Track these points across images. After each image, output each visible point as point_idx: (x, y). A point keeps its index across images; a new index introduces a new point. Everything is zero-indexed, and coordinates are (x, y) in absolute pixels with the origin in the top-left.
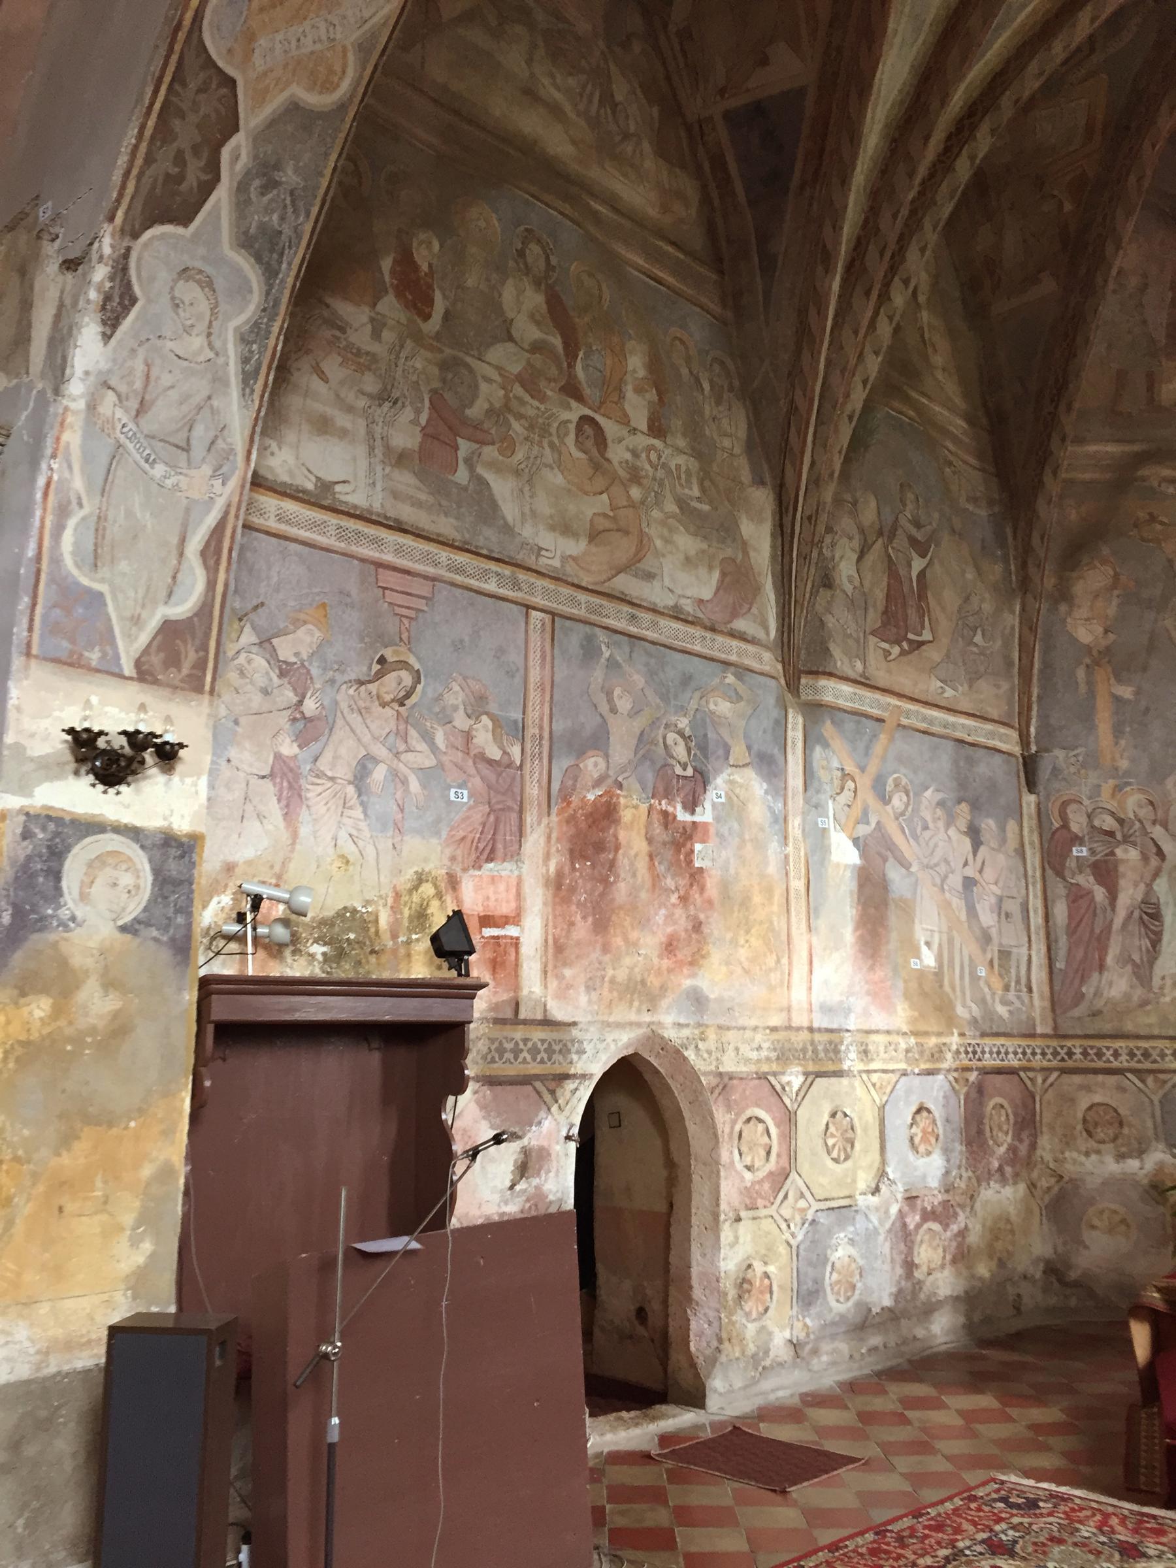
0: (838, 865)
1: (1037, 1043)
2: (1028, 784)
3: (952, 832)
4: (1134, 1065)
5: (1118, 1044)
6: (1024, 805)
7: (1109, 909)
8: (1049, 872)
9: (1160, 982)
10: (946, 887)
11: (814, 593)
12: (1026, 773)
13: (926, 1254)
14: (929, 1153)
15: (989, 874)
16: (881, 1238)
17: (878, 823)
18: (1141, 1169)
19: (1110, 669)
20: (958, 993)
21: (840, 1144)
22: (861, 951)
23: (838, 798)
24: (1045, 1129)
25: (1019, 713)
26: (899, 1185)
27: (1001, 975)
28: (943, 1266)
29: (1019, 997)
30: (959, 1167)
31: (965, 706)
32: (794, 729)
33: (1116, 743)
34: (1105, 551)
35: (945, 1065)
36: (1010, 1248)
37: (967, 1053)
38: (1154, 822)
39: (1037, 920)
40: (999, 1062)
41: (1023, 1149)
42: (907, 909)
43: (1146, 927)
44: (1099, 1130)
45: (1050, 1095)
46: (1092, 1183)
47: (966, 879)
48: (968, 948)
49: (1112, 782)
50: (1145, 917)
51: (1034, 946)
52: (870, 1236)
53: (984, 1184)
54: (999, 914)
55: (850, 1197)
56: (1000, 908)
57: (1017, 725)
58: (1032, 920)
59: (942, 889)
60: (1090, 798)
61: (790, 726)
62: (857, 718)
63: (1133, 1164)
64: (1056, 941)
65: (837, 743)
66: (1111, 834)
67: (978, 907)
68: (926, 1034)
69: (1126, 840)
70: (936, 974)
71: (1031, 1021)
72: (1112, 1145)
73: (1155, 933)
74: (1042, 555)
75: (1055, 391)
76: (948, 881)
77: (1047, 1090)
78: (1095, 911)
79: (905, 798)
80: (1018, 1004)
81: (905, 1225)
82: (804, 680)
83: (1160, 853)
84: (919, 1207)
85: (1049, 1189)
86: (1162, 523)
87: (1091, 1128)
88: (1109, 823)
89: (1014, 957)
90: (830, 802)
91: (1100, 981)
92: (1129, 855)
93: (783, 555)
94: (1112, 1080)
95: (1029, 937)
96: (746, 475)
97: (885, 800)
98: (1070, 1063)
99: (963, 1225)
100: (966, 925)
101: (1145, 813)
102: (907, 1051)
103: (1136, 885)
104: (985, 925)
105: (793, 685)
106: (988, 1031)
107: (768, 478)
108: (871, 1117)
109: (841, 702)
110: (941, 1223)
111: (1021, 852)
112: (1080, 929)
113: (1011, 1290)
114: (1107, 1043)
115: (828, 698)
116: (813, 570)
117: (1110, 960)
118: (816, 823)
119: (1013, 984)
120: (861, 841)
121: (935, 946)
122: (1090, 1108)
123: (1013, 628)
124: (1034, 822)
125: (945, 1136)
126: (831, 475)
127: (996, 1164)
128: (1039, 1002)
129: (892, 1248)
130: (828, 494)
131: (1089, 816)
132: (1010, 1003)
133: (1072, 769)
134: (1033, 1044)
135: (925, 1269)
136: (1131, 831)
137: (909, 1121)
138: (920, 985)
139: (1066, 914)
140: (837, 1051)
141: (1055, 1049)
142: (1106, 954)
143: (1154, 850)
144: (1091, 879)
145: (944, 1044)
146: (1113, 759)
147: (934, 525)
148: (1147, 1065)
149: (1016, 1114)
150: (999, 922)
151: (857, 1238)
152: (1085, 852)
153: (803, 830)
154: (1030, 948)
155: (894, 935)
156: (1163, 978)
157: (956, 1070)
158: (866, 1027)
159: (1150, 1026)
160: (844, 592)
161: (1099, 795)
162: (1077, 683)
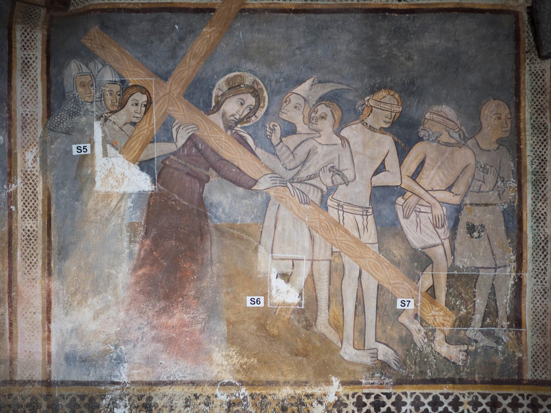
0: (108, 196)
6: (527, 78)
23: (113, 117)
51: (529, 265)
54: (454, 229)
56: (457, 222)
90: (97, 126)
119: (478, 317)
120: (156, 164)
132: (469, 341)
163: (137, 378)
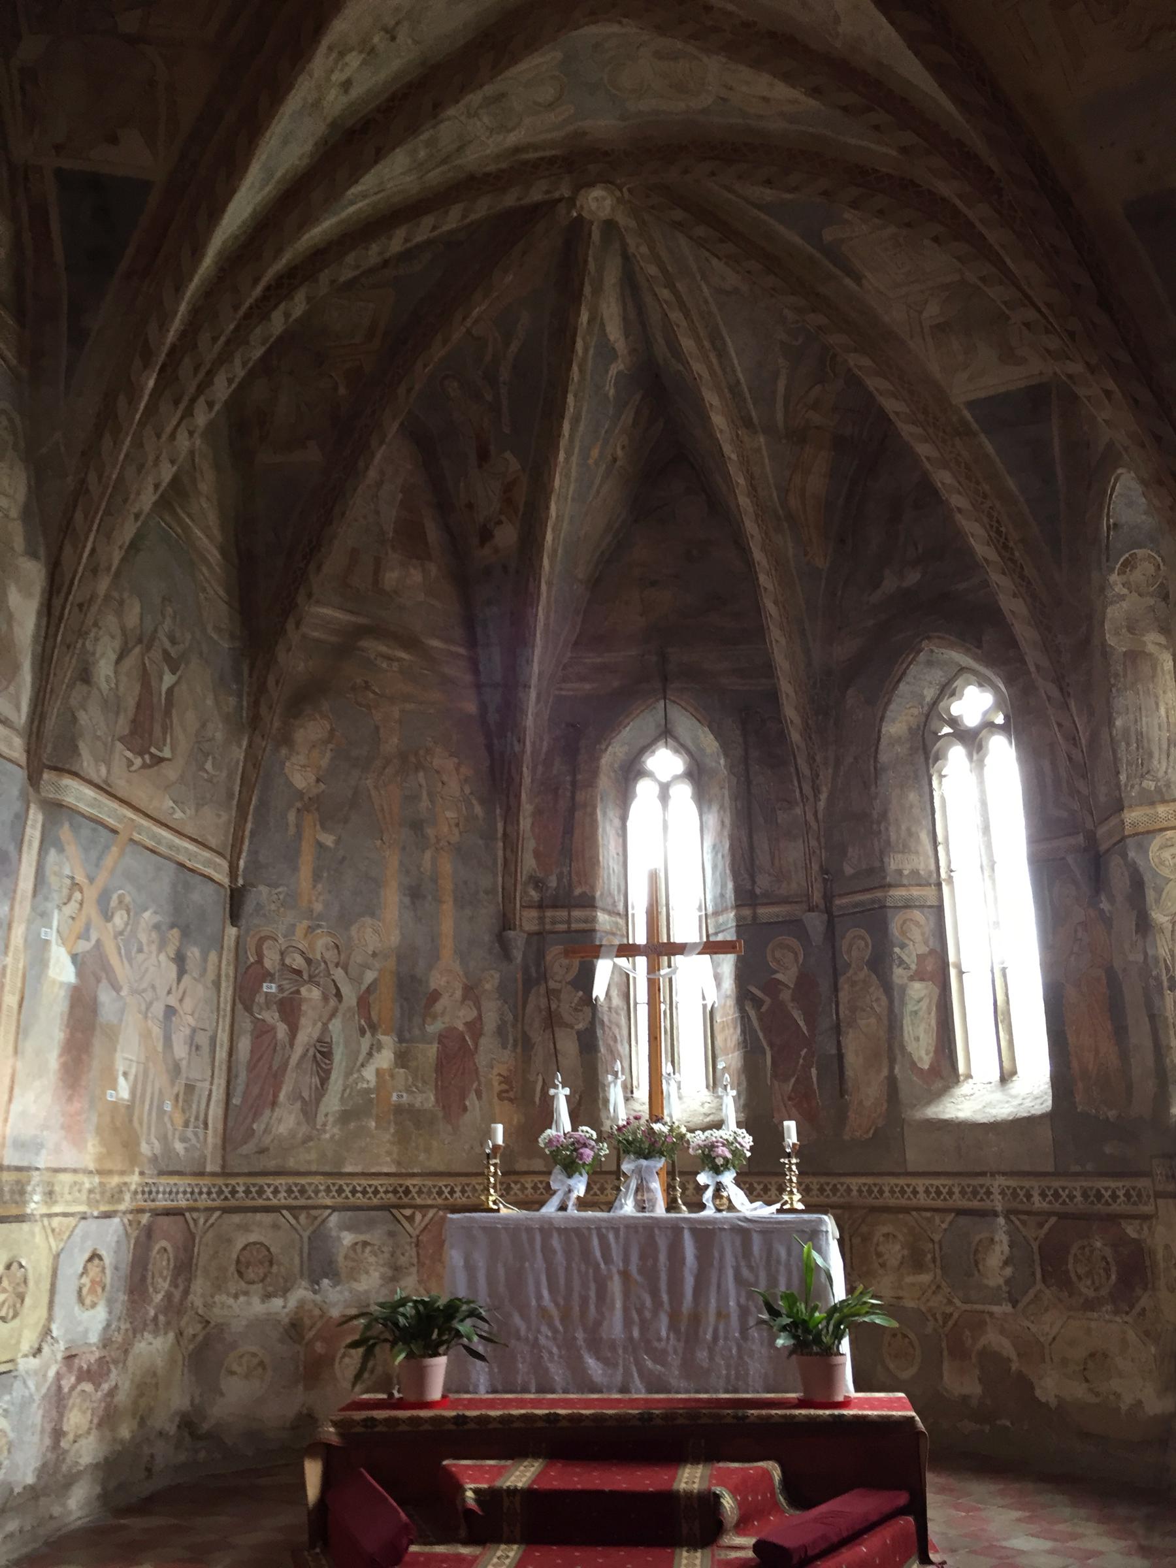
0: (54, 982)
1: (205, 1182)
2: (231, 917)
3: (162, 957)
4: (290, 1202)
5: (280, 1181)
7: (288, 1046)
8: (239, 1006)
9: (323, 1119)
10: (150, 1015)
11: (71, 686)
12: (231, 905)
13: (77, 1419)
14: (94, 1305)
15: (188, 1004)
16: (35, 1405)
17: (98, 941)
18: (284, 1307)
20: (145, 1126)
21: (10, 1302)
22: (61, 1079)
23: (64, 908)
24: (199, 1272)
25: (233, 846)
26: (61, 1342)
27: (183, 1111)
28: (89, 1432)
29: (196, 1134)
30: (120, 1318)
31: (189, 830)
32: (33, 827)
33: (314, 887)
35: (122, 1207)
36: (152, 1404)
37: (143, 1193)
38: (337, 965)
39: (222, 1054)
40: (169, 1203)
41: (177, 1295)
42: (112, 1035)
43: (318, 1065)
44: (250, 1270)
45: (210, 1234)
46: (237, 1326)
47: (168, 1006)
48: (159, 1080)
49: (305, 923)
50: (318, 1055)
51: (216, 1081)
52: (25, 1404)
53: (138, 1336)
54: (191, 1045)
55: (11, 1361)
58: (217, 1053)
59: (146, 1017)
60: (285, 937)
61: (29, 823)
62: (93, 825)
63: (278, 1302)
64: (237, 1076)
65: (72, 849)
66: (298, 972)
67: (174, 1037)
68: (110, 1173)
69: (312, 980)
70: (128, 1107)
71: (203, 1161)
72: (261, 1285)
73: (325, 1071)
76: (152, 1009)
77: (208, 1230)
78: (275, 1050)
79: (126, 916)
80: (194, 1141)
81: (60, 1388)
82: (46, 776)
83: (339, 995)
84: (76, 1366)
85: (194, 1336)
86: (374, 692)
87: (243, 1270)
88: (298, 962)
89: (197, 1092)
90: (56, 913)
91: (271, 1118)
92: (312, 994)
93: (46, 638)
94: (267, 1218)
95: (213, 1074)
96: (19, 543)
97: (108, 916)
98: (233, 1202)
99: (113, 1383)
100: (161, 1055)
101: (331, 955)
102: (91, 1191)
103: (314, 1024)
104: (177, 1057)
105: (34, 779)
106: (165, 1169)
107: (42, 551)
108: (45, 1267)
109: (83, 807)
110: (94, 1384)
111: (217, 984)
112: (261, 1064)
113: (146, 1450)
114: (269, 1180)
115: (70, 800)
116: (74, 661)
117: (282, 1096)
118: (39, 934)
119: (192, 1119)
120: (79, 958)
121: (131, 1078)
122: (244, 1248)
124: (232, 955)
125: (112, 1286)
126: (109, 569)
127: (152, 1313)
128: (212, 1138)
129: (43, 1416)
130: (103, 585)
131: (282, 954)
133: (273, 907)
134: (201, 1183)
135: (71, 1437)
136: (317, 972)
137: (80, 1270)
138: (113, 1118)
139: (249, 1048)
140: (22, 1192)
141: (220, 1187)
142: (280, 1088)
143: (334, 991)
144: (277, 1015)
145: (125, 1184)
146: (310, 901)
147: (187, 644)
148: (302, 1202)
149: (176, 1258)
150: (189, 1054)
151: (12, 1409)
152: (273, 988)
153: (26, 940)
154: (212, 1084)
155: (96, 1064)
156: (326, 1115)
157: (131, 1212)
158: (55, 1165)
159: (309, 1162)
160: (99, 689)
161: (294, 934)
162: (287, 824)
163: (49, 1165)
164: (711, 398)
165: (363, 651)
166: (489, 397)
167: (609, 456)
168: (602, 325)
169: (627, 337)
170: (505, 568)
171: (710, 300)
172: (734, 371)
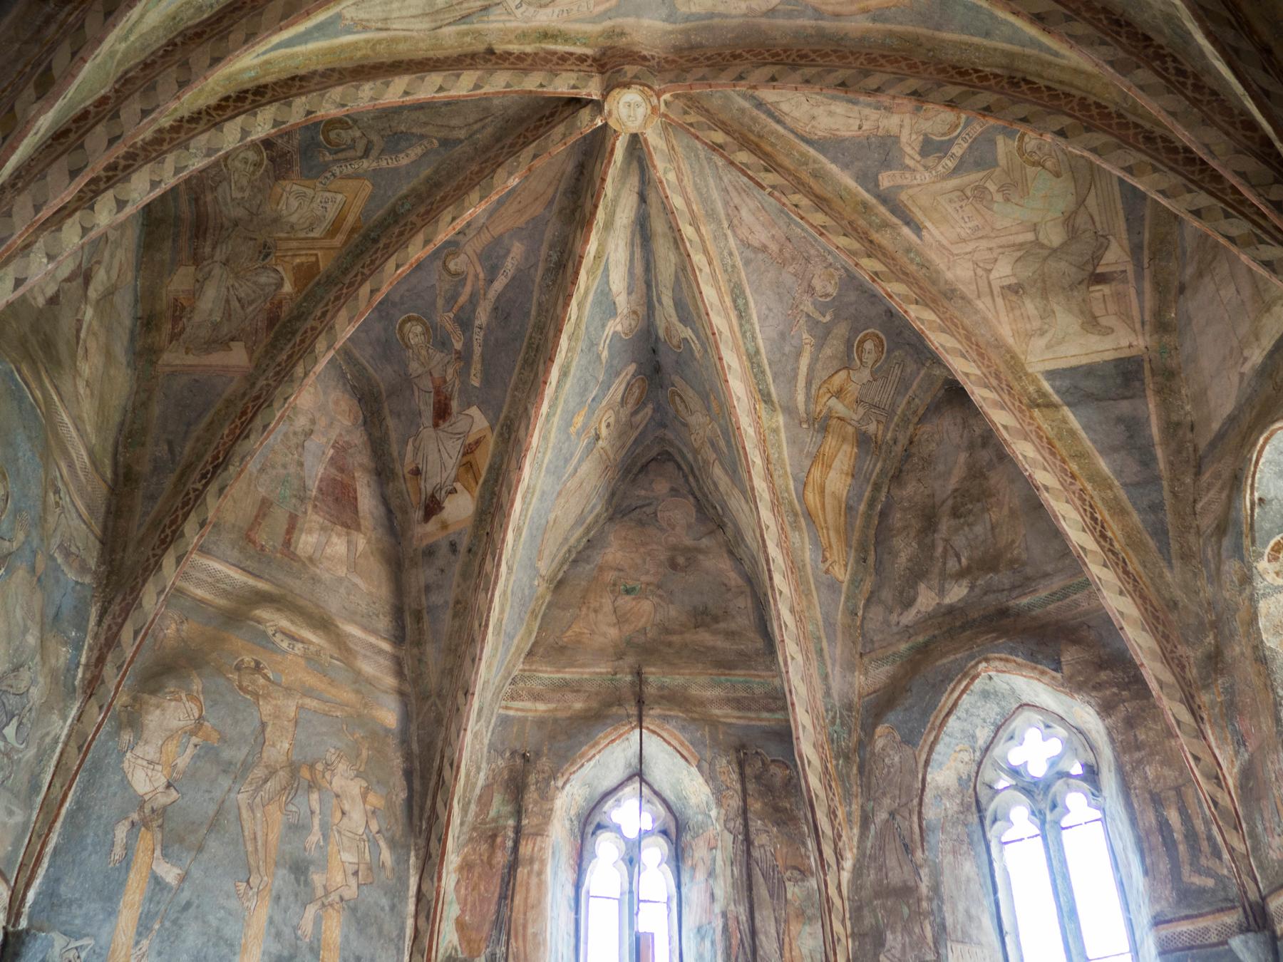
19: (159, 836)
34: (197, 685)
57: (12, 883)
74: (129, 654)
75: (210, 468)
86: (265, 677)
123: (56, 741)
164: (731, 359)
165: (259, 623)
166: (458, 346)
167: (593, 432)
168: (606, 269)
169: (629, 294)
170: (453, 547)
171: (736, 253)
172: (754, 338)
